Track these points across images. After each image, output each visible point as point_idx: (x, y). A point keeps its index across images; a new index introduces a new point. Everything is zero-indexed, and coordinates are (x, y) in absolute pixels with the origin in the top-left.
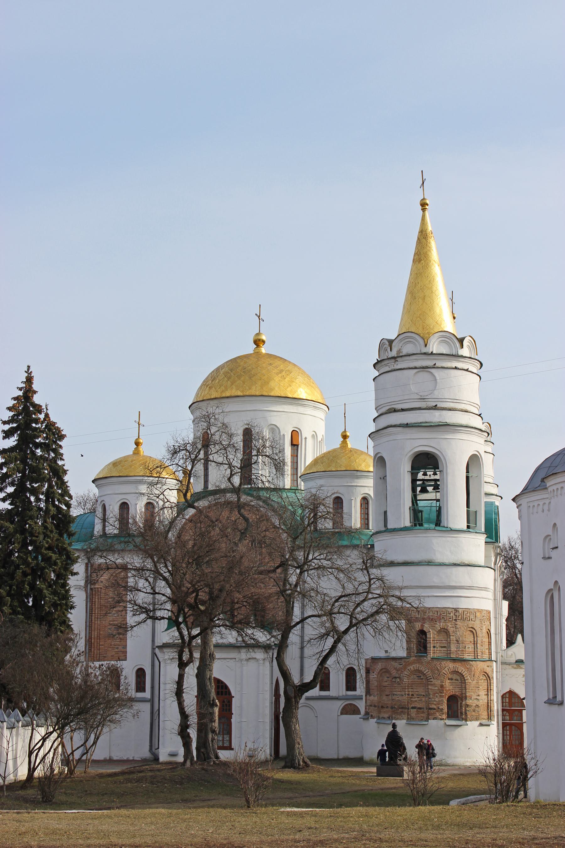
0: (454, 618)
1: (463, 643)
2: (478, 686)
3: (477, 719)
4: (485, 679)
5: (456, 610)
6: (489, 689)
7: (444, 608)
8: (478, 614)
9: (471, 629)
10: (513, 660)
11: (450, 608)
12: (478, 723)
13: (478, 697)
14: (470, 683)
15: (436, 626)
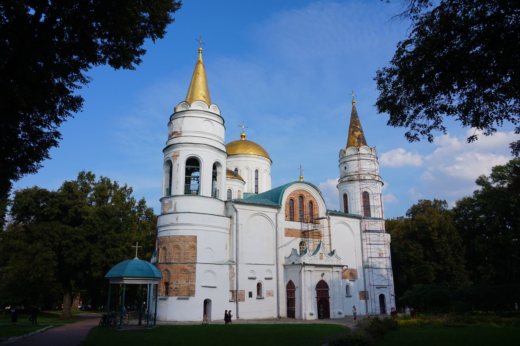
0: (168, 241)
1: (172, 254)
2: (177, 277)
3: (176, 295)
4: (186, 273)
5: (169, 237)
6: (189, 278)
7: (165, 236)
8: (181, 238)
9: (177, 246)
10: (291, 263)
11: (167, 236)
12: (177, 297)
13: (177, 283)
14: (172, 275)
15: (162, 246)
